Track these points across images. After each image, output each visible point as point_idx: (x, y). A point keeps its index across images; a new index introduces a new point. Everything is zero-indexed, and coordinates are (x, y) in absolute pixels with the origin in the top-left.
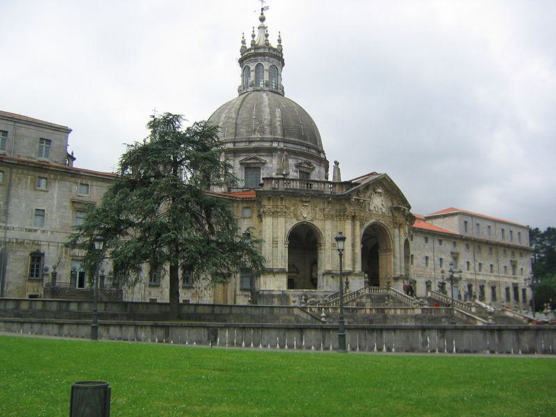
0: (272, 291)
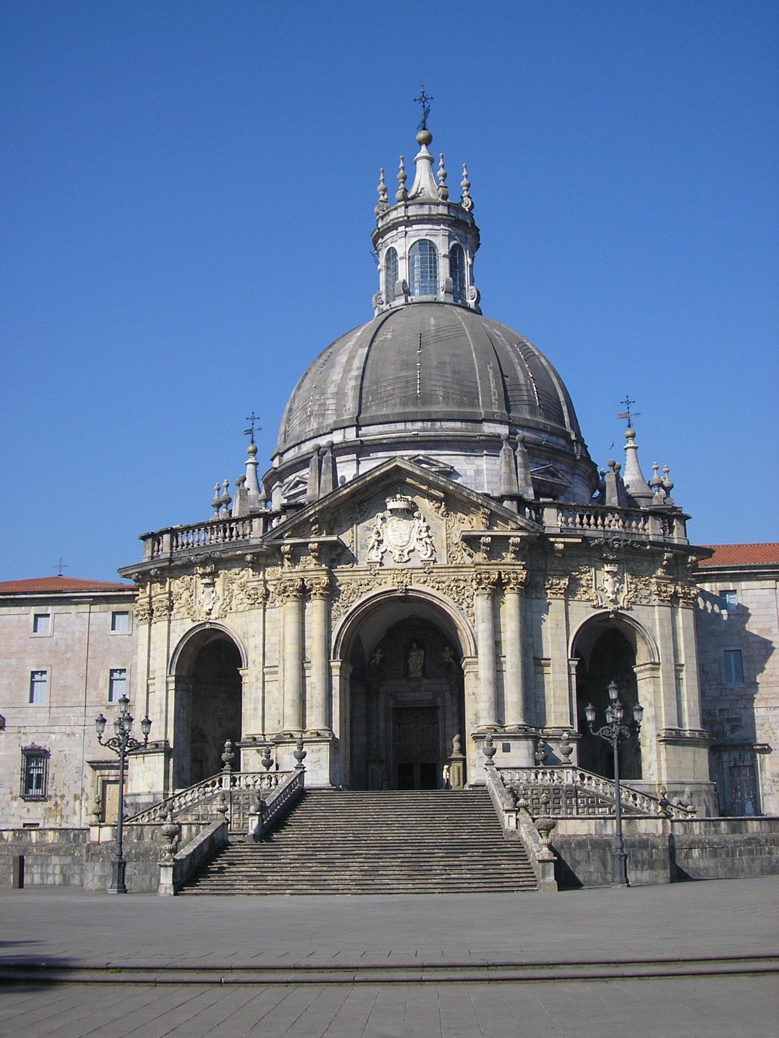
0: (139, 795)
